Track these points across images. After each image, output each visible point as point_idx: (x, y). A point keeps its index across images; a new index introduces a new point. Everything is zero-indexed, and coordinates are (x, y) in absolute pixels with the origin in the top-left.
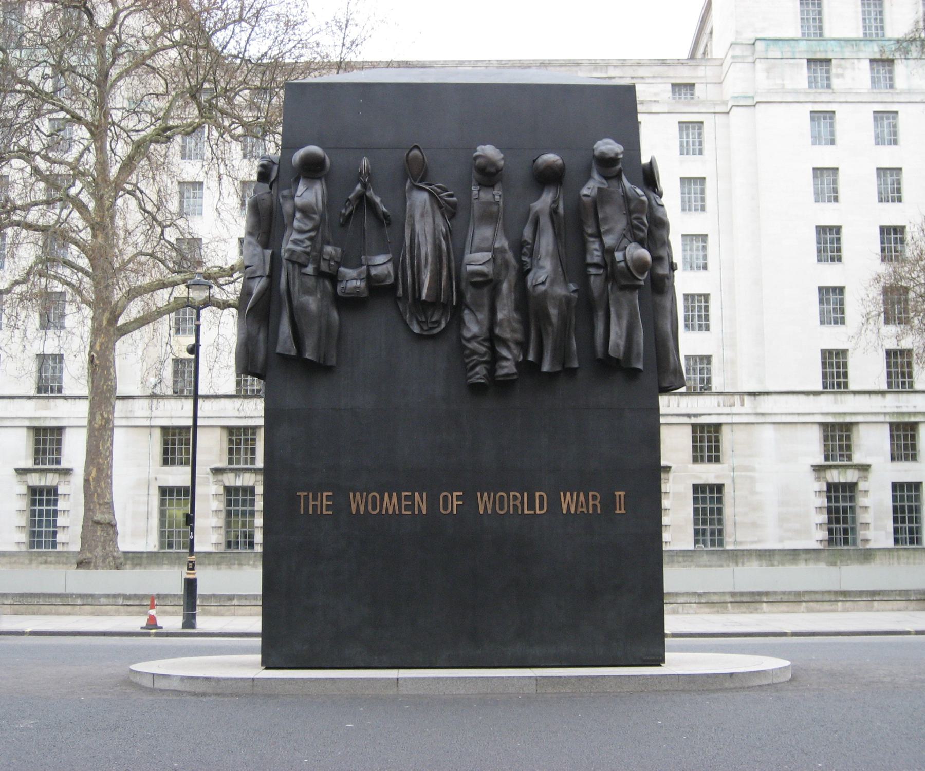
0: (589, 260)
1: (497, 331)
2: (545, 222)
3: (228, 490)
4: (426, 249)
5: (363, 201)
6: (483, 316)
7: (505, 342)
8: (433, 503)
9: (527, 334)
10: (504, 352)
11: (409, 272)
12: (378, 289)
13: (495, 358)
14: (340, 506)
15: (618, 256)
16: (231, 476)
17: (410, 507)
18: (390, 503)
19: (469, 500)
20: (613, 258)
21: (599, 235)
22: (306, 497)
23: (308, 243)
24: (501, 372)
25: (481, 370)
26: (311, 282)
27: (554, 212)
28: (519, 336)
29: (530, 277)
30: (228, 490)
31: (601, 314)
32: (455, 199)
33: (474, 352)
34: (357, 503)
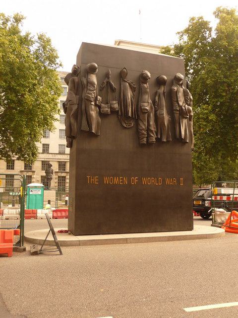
0: (174, 109)
1: (151, 128)
2: (162, 96)
3: (59, 177)
4: (129, 100)
5: (108, 83)
6: (146, 123)
7: (152, 131)
8: (129, 181)
9: (157, 129)
10: (152, 135)
11: (123, 108)
12: (113, 111)
13: (149, 136)
14: (101, 181)
15: (183, 108)
16: (60, 173)
17: (122, 182)
18: (116, 181)
19: (140, 180)
20: (182, 108)
21: (177, 102)
22: (90, 178)
23: (93, 94)
24: (150, 141)
25: (145, 139)
26: (93, 107)
27: (164, 93)
28: (155, 130)
29: (158, 112)
30: (59, 177)
31: (178, 125)
32: (135, 86)
33: (143, 134)
34: (106, 180)
